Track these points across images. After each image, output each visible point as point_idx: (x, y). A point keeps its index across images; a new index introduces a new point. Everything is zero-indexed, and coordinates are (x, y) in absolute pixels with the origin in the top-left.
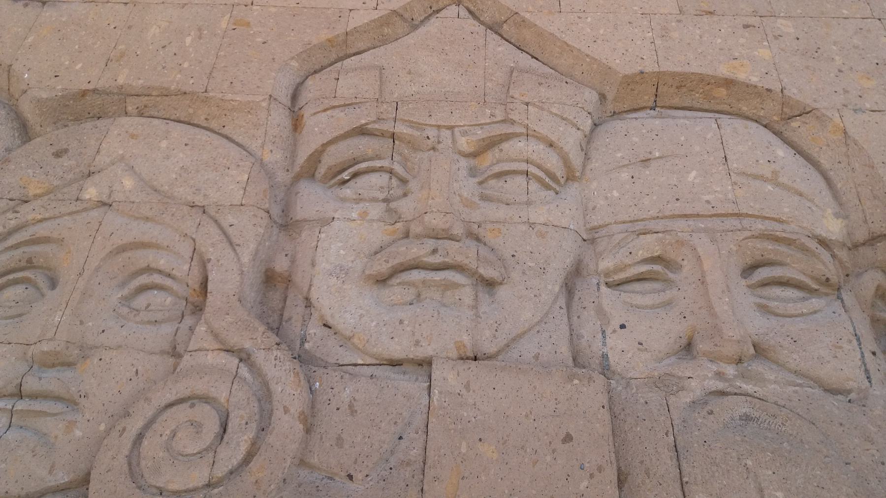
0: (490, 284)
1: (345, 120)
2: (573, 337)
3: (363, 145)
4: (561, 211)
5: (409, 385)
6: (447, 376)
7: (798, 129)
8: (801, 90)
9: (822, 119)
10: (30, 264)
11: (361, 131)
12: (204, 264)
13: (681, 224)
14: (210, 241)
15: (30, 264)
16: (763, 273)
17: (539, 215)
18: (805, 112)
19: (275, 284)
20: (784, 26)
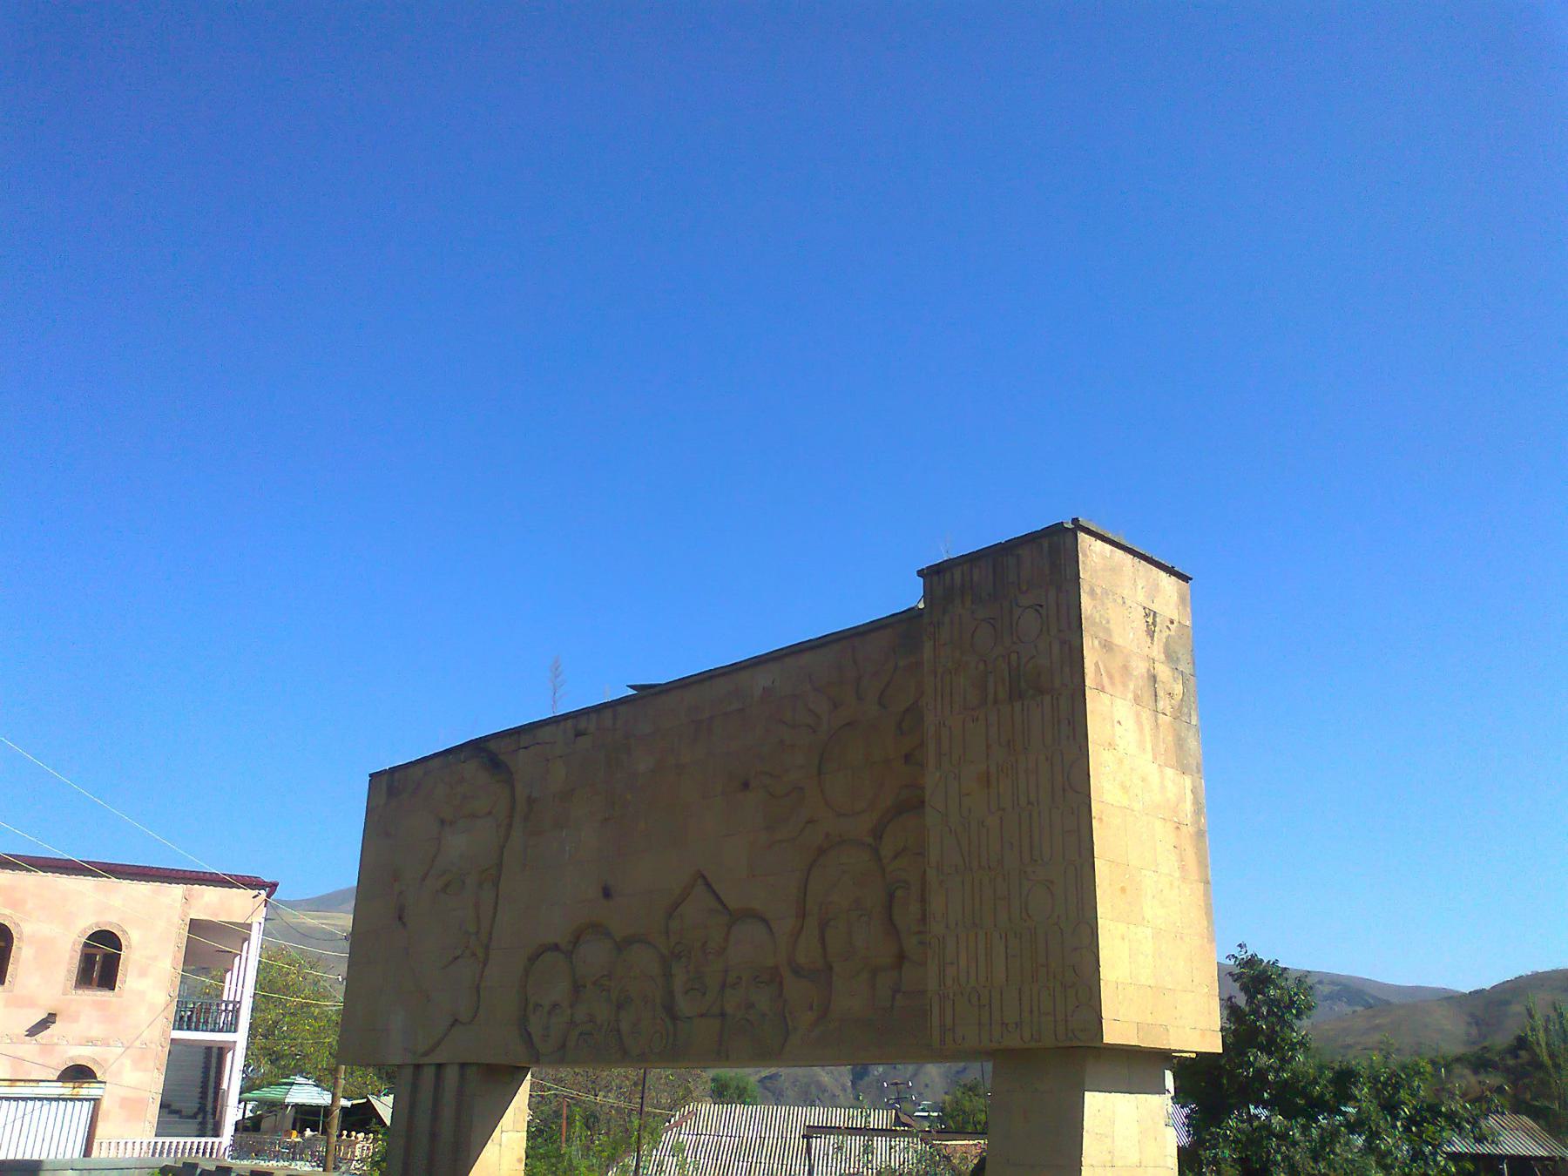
19: (671, 993)
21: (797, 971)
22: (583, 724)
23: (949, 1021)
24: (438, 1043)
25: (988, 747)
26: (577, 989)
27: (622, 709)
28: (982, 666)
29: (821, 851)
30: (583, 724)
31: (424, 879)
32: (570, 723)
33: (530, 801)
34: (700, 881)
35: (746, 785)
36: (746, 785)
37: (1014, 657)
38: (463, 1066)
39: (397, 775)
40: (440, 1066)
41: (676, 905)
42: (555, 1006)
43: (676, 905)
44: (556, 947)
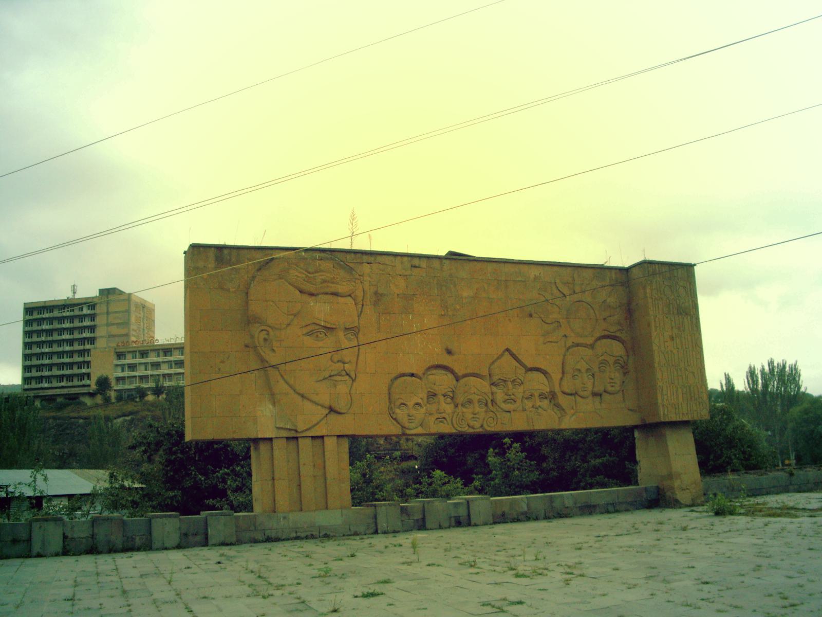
0: (515, 402)
1: (497, 377)
2: (522, 406)
3: (500, 381)
4: (521, 389)
5: (508, 414)
6: (512, 413)
7: (547, 375)
8: (548, 371)
9: (550, 375)
10: (468, 402)
11: (500, 379)
12: (487, 401)
13: (533, 391)
14: (487, 397)
15: (468, 402)
16: (541, 396)
17: (520, 390)
18: (548, 373)
20: (548, 357)
21: (564, 393)
22: (416, 262)
23: (666, 413)
24: (316, 425)
25: (672, 328)
26: (432, 395)
27: (444, 261)
28: (668, 301)
29: (569, 348)
30: (416, 262)
31: (288, 325)
32: (405, 259)
33: (376, 293)
34: (507, 353)
35: (531, 315)
36: (531, 315)
37: (678, 301)
38: (339, 436)
39: (226, 252)
40: (313, 437)
41: (493, 363)
42: (418, 404)
43: (493, 363)
44: (412, 375)
